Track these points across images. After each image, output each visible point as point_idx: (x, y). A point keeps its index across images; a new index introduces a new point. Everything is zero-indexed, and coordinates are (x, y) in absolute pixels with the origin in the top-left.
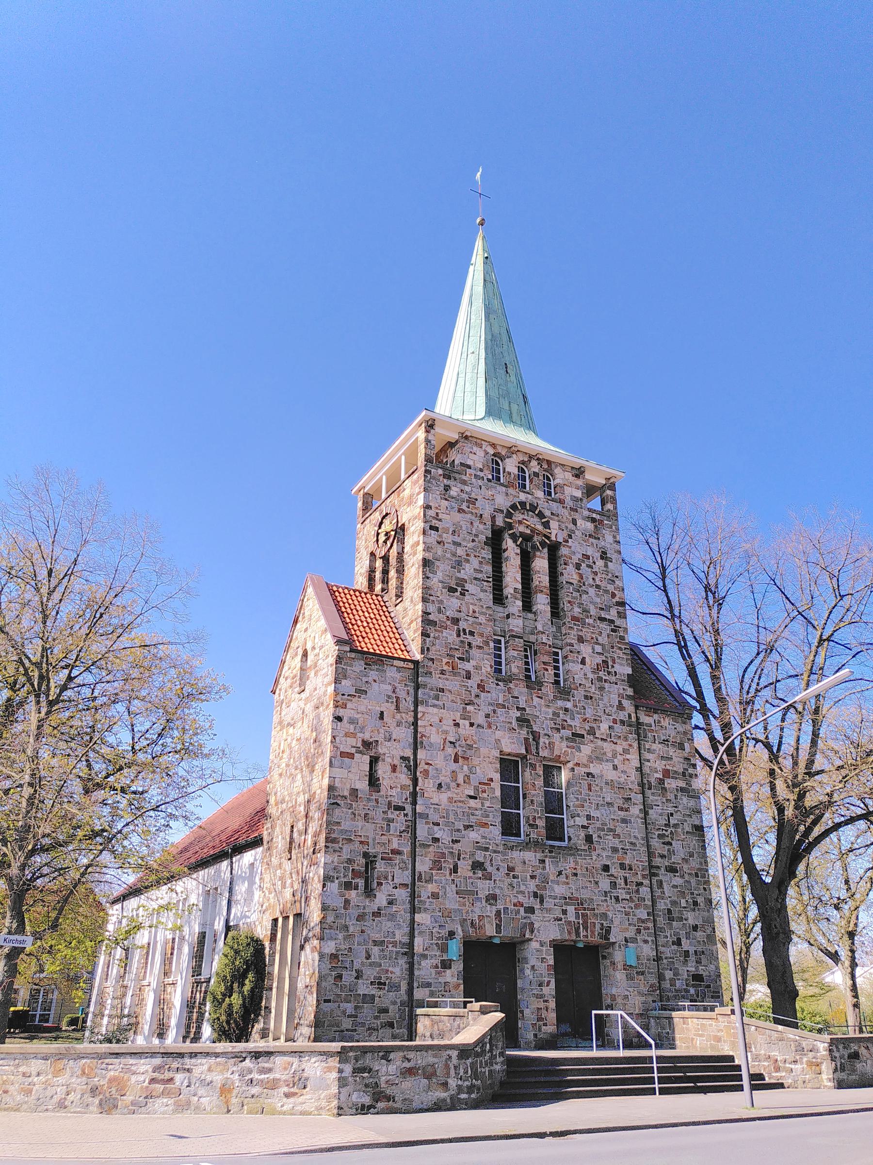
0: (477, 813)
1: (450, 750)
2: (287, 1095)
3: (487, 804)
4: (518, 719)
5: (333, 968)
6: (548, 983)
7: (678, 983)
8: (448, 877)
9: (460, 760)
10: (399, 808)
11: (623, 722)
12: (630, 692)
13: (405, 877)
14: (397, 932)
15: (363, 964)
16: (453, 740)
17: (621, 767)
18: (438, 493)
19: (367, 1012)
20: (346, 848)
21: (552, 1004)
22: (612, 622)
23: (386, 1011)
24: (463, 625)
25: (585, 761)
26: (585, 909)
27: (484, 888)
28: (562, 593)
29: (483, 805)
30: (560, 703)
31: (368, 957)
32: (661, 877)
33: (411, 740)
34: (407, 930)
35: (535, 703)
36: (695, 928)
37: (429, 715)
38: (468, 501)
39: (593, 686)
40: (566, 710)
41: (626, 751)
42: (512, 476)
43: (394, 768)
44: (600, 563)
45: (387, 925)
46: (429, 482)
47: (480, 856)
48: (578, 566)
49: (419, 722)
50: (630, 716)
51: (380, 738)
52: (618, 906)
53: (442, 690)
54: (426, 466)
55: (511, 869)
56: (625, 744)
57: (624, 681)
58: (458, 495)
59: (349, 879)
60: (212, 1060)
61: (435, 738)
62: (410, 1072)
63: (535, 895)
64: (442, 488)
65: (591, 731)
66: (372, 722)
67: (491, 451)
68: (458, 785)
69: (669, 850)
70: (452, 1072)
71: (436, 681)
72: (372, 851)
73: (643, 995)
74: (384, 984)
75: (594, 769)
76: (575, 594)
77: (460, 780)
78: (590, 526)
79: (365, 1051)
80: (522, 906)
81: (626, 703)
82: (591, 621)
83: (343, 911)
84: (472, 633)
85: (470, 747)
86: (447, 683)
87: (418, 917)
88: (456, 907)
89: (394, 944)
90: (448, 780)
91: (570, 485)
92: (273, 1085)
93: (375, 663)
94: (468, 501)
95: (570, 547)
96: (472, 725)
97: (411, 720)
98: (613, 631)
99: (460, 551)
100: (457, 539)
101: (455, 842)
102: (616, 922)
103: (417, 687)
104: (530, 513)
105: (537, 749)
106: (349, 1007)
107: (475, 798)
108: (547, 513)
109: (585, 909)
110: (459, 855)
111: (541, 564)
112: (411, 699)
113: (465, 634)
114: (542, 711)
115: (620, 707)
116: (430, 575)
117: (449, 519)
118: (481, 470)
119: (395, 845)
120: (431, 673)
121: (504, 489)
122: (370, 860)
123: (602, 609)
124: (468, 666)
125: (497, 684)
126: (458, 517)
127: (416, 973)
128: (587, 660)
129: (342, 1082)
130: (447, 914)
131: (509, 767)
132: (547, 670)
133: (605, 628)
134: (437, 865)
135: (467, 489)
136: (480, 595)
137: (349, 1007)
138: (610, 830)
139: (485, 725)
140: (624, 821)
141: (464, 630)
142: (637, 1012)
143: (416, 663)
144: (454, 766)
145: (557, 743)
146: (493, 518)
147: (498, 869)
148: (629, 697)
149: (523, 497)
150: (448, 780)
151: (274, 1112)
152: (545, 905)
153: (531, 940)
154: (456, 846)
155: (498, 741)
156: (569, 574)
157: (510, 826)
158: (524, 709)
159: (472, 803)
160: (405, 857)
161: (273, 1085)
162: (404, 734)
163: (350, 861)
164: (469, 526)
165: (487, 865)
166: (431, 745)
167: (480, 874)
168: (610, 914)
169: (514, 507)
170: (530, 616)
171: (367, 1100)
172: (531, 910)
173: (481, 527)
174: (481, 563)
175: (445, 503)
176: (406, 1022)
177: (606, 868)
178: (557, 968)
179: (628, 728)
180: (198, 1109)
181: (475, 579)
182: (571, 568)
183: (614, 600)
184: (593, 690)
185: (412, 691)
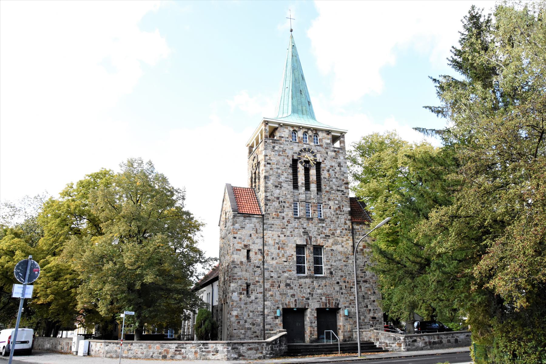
1: (277, 246)
2: (213, 355)
3: (291, 263)
4: (303, 232)
5: (237, 320)
7: (366, 321)
10: (258, 267)
11: (346, 229)
12: (349, 217)
13: (261, 290)
17: (345, 246)
19: (249, 333)
20: (239, 282)
21: (316, 329)
22: (343, 191)
23: (256, 332)
24: (281, 199)
25: (330, 245)
28: (322, 182)
30: (320, 225)
31: (249, 316)
36: (374, 301)
40: (323, 227)
41: (347, 240)
43: (256, 253)
44: (338, 168)
45: (255, 306)
48: (328, 171)
51: (250, 243)
52: (342, 296)
53: (273, 224)
55: (300, 285)
56: (347, 238)
60: (191, 345)
61: (271, 242)
62: (251, 349)
63: (310, 294)
65: (333, 234)
66: (247, 238)
67: (292, 129)
71: (271, 221)
72: (249, 282)
75: (334, 248)
77: (281, 255)
78: (333, 154)
79: (235, 343)
81: (348, 222)
82: (333, 192)
84: (285, 202)
85: (284, 244)
89: (258, 312)
92: (209, 352)
96: (285, 236)
97: (262, 236)
98: (343, 194)
99: (279, 171)
100: (278, 166)
101: (278, 277)
103: (264, 224)
106: (243, 331)
108: (315, 151)
111: (313, 172)
112: (261, 229)
114: (313, 229)
115: (345, 224)
117: (274, 159)
119: (257, 279)
122: (248, 286)
123: (338, 187)
126: (279, 158)
128: (332, 207)
129: (228, 351)
130: (277, 301)
131: (300, 249)
134: (272, 285)
135: (282, 146)
136: (288, 187)
140: (345, 266)
143: (263, 215)
144: (278, 251)
146: (293, 156)
148: (349, 220)
149: (305, 146)
151: (209, 359)
152: (314, 297)
153: (307, 309)
155: (295, 241)
156: (324, 174)
157: (300, 270)
159: (285, 263)
160: (261, 283)
161: (209, 352)
162: (260, 241)
163: (241, 286)
165: (291, 284)
166: (269, 245)
167: (288, 287)
168: (339, 299)
169: (301, 151)
170: (309, 192)
171: (236, 356)
172: (308, 299)
173: (288, 160)
175: (273, 153)
177: (338, 283)
178: (318, 318)
180: (189, 359)
182: (325, 172)
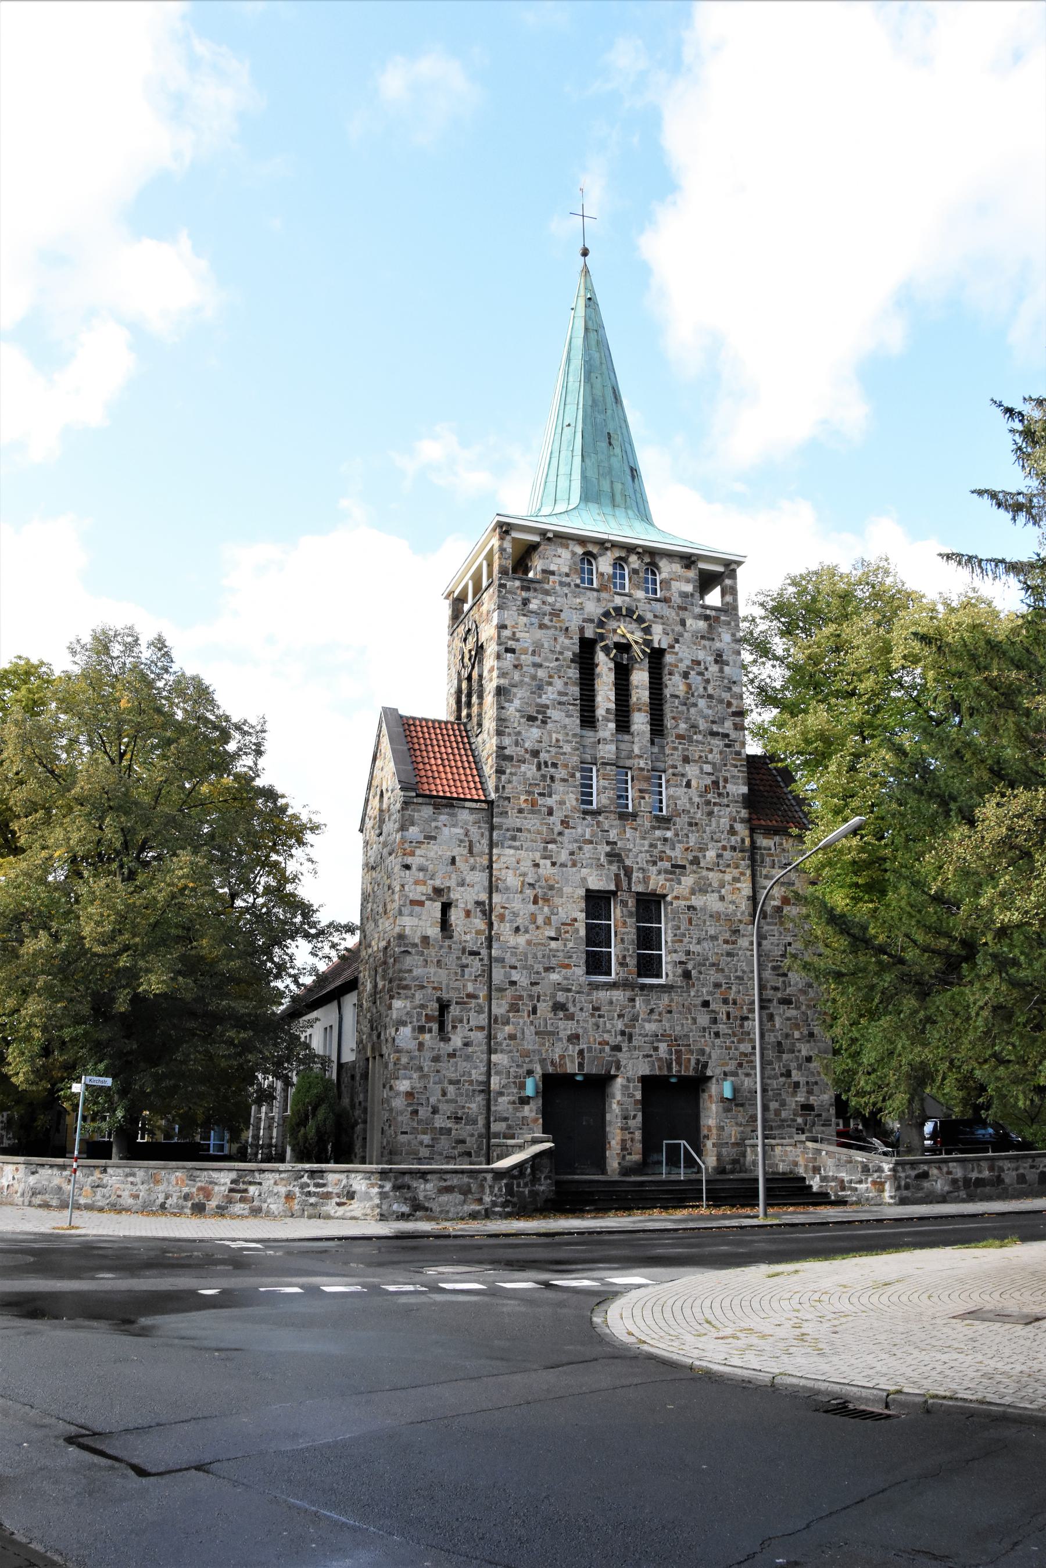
0: (559, 954)
1: (529, 893)
2: (339, 1204)
3: (570, 945)
4: (608, 855)
5: (409, 1105)
6: (635, 1117)
7: (784, 1114)
8: (526, 1018)
9: (540, 902)
10: (473, 953)
11: (734, 849)
12: (744, 813)
13: (483, 1020)
14: (473, 1072)
15: (439, 1101)
16: (531, 881)
17: (729, 898)
18: (515, 608)
19: (444, 1144)
20: (419, 995)
21: (638, 1135)
22: (727, 736)
23: (463, 1142)
24: (544, 756)
25: (686, 892)
26: (679, 1045)
27: (566, 1028)
28: (667, 708)
29: (565, 945)
30: (658, 833)
31: (444, 1094)
32: (771, 1010)
33: (487, 884)
34: (484, 1069)
35: (628, 836)
36: (809, 1059)
37: (505, 856)
38: (551, 614)
39: (699, 811)
40: (665, 840)
41: (736, 880)
42: (606, 577)
43: (468, 914)
44: (714, 668)
45: (463, 1065)
46: (504, 598)
47: (561, 997)
48: (686, 675)
49: (494, 866)
50: (743, 841)
51: (452, 883)
52: (718, 1041)
53: (520, 830)
54: (500, 579)
55: (596, 1009)
56: (736, 873)
57: (737, 802)
58: (540, 608)
59: (423, 1022)
60: (277, 1176)
61: (512, 880)
62: (449, 1190)
63: (623, 1033)
64: (519, 603)
65: (696, 861)
66: (443, 869)
67: (579, 550)
68: (538, 928)
69: (784, 982)
70: (487, 1191)
71: (513, 820)
72: (445, 996)
73: (741, 1125)
74: (461, 1118)
75: (697, 901)
76: (681, 708)
77: (540, 920)
78: (702, 624)
79: (403, 1173)
80: (608, 1044)
81: (739, 827)
82: (700, 737)
83: (417, 1053)
84: (555, 765)
85: (551, 888)
86: (525, 822)
87: (494, 1057)
88: (536, 1047)
89: (471, 1082)
90: (527, 923)
91: (679, 578)
92: (328, 1196)
93: (446, 806)
94: (551, 614)
95: (677, 654)
96: (554, 864)
97: (486, 863)
98: (727, 746)
99: (541, 673)
100: (537, 659)
101: (532, 984)
102: (714, 1056)
103: (492, 828)
104: (628, 619)
105: (629, 884)
106: (426, 1139)
107: (556, 939)
108: (649, 616)
109: (679, 1045)
110: (539, 997)
111: (640, 677)
112: (485, 841)
113: (546, 766)
114: (636, 844)
115: (732, 831)
116: (507, 705)
117: (527, 638)
118: (567, 575)
119: (470, 988)
120: (507, 813)
121: (595, 594)
122: (444, 1007)
123: (713, 722)
124: (550, 801)
125: (584, 819)
126: (539, 634)
127: (493, 1108)
128: (694, 783)
129: (383, 1195)
130: (526, 1054)
131: (597, 903)
132: (644, 798)
133: (717, 743)
134: (514, 1008)
135: (550, 599)
136: (565, 719)
137: (426, 1139)
138: (713, 965)
139: (570, 864)
140: (729, 954)
141: (546, 763)
142: (733, 1140)
143: (491, 803)
144: (532, 908)
145: (653, 877)
146: (582, 629)
147: (581, 1009)
148: (742, 821)
149: (618, 601)
150: (527, 923)
151: (328, 1217)
152: (635, 1043)
153: (616, 1076)
154: (534, 988)
155: (584, 880)
156: (674, 685)
157: (597, 964)
158: (615, 843)
159: (553, 944)
160: (481, 1001)
161: (328, 1196)
162: (479, 878)
163: (423, 1006)
164: (552, 643)
165: (570, 1005)
166: (507, 889)
167: (561, 1014)
168: (707, 1049)
169: (606, 614)
170: (627, 737)
171: (405, 1209)
172: (617, 1048)
173: (567, 641)
174: (566, 684)
175: (523, 620)
176: (484, 1152)
177: (706, 1004)
178: (646, 1104)
179: (740, 855)
180: (269, 1214)
181: (560, 703)
182: (677, 678)
183: (730, 710)
184: (699, 815)
185: (487, 833)
